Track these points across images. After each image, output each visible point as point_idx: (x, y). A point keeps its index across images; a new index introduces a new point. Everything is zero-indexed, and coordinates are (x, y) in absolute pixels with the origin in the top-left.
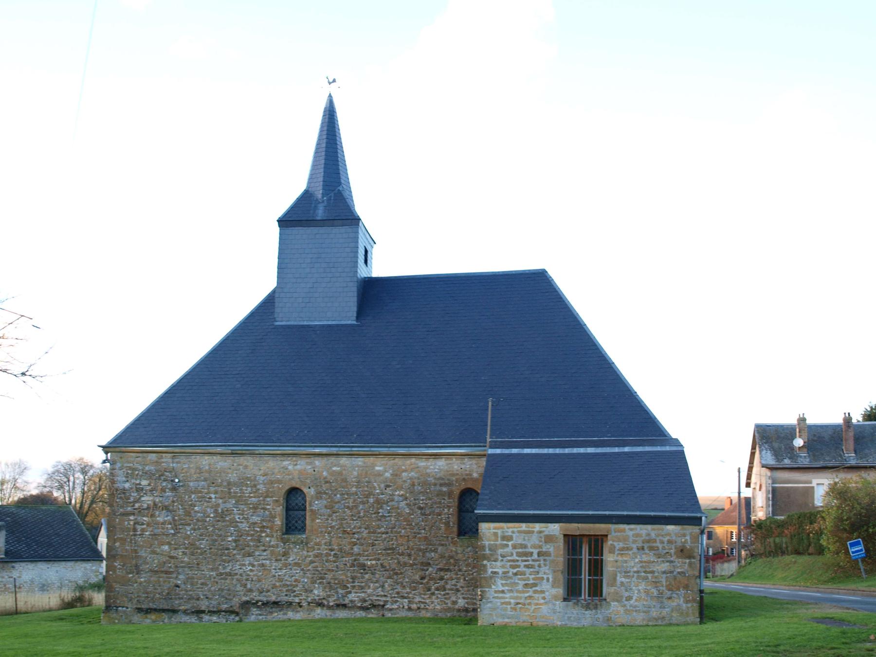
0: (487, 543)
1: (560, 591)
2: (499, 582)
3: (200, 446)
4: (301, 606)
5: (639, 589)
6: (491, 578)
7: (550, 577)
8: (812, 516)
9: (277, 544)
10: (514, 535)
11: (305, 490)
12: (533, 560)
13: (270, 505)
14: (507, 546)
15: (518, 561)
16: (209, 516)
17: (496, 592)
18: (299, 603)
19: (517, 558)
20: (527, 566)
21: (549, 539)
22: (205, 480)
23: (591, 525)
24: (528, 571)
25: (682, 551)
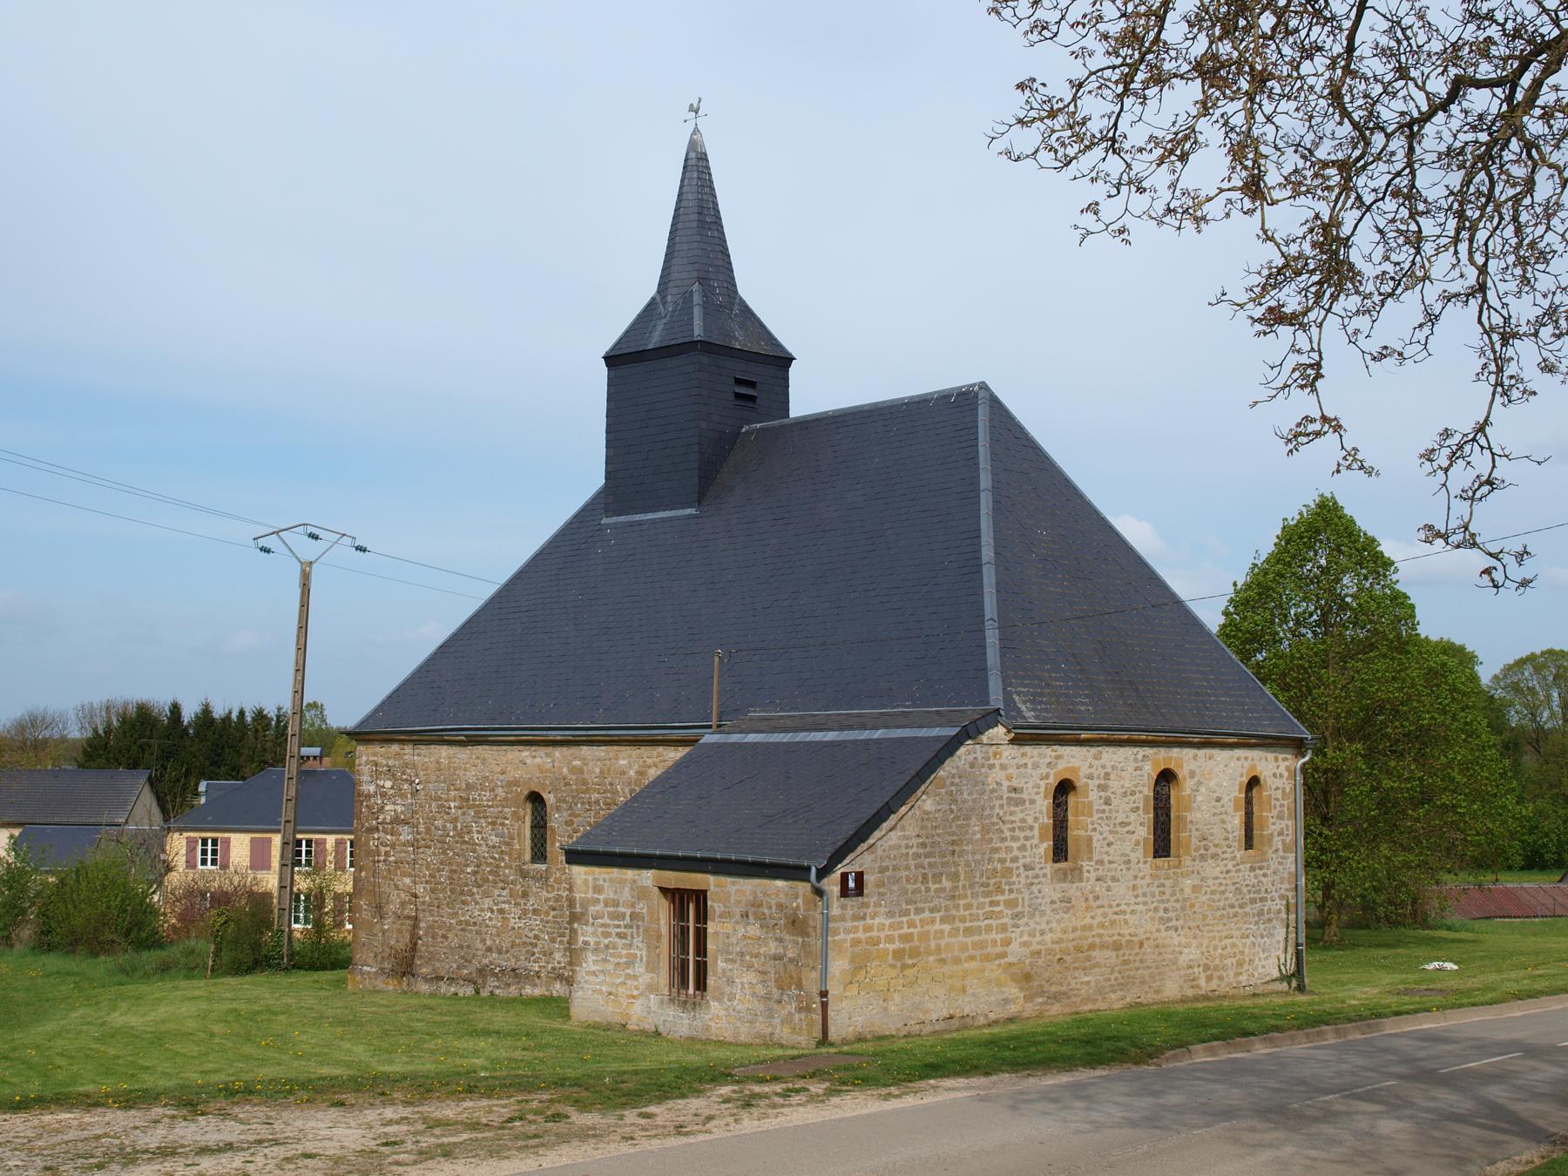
0: (578, 896)
1: (663, 978)
2: (591, 957)
3: (415, 731)
4: (539, 977)
5: (746, 983)
6: (582, 949)
7: (644, 953)
8: (267, 896)
9: (516, 880)
10: (606, 885)
11: (545, 796)
12: (626, 927)
13: (507, 819)
14: (598, 901)
15: (609, 926)
16: (448, 836)
17: (588, 973)
18: (538, 972)
19: (608, 921)
20: (619, 935)
21: (642, 894)
22: (444, 782)
23: (686, 874)
24: (620, 942)
25: (794, 921)
